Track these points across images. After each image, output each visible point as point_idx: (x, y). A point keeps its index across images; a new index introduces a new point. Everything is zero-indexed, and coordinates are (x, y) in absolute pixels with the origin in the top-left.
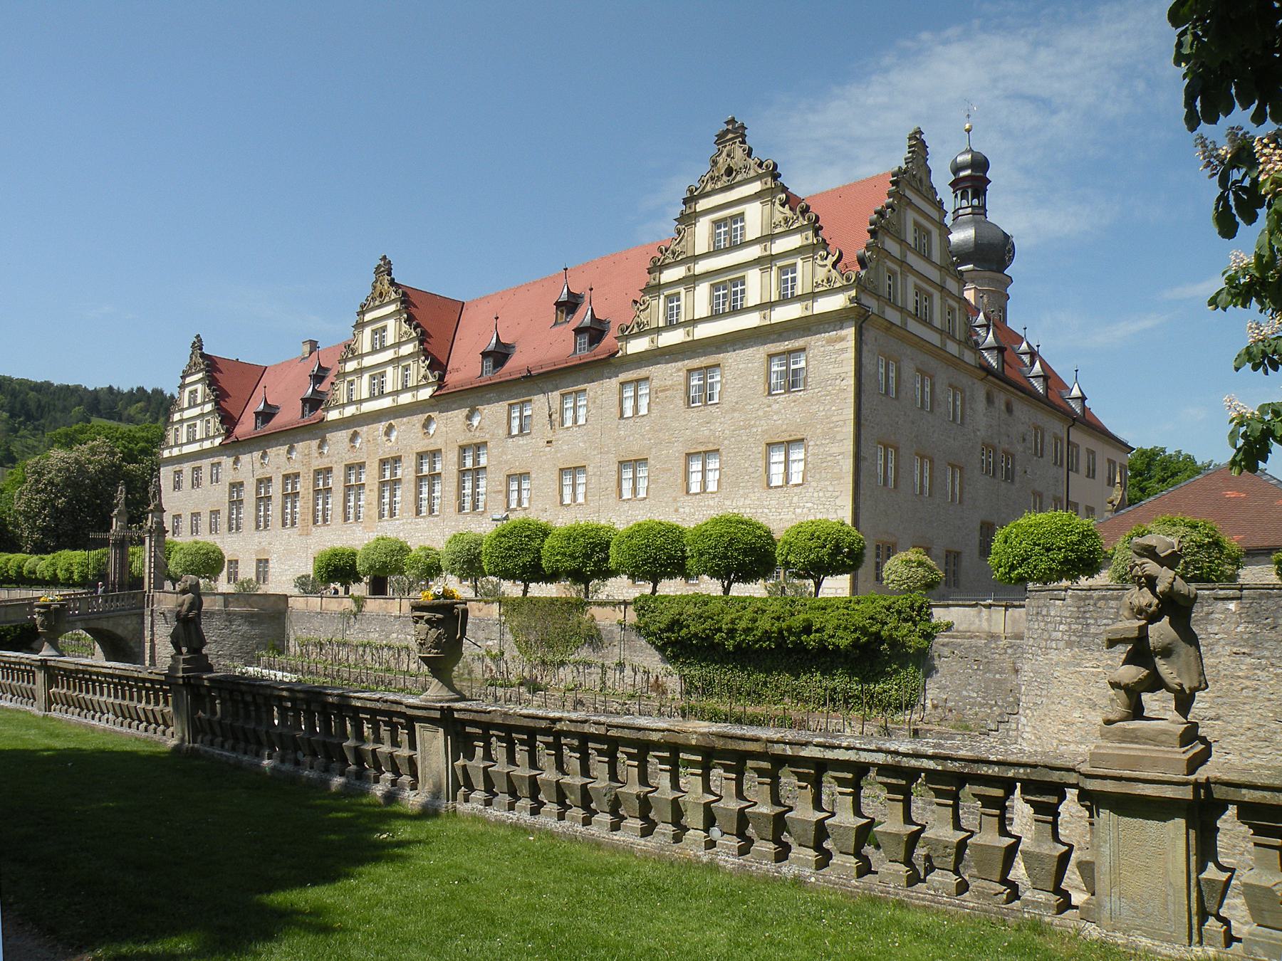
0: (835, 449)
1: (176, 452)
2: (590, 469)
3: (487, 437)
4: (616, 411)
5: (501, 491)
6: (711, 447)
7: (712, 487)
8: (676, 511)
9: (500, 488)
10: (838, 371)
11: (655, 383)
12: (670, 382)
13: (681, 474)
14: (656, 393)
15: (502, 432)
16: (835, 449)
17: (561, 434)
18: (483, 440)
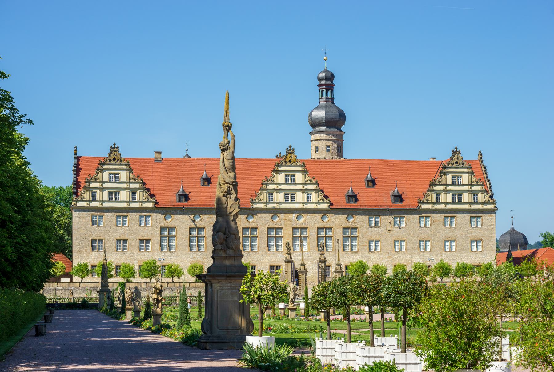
0: (491, 243)
1: (84, 204)
2: (407, 241)
3: (358, 226)
4: (418, 224)
5: (366, 245)
6: (453, 239)
7: (454, 250)
8: (442, 256)
9: (365, 244)
10: (491, 224)
11: (433, 218)
12: (438, 219)
13: (443, 245)
14: (433, 221)
15: (366, 225)
16: (491, 243)
17: (394, 229)
18: (356, 227)
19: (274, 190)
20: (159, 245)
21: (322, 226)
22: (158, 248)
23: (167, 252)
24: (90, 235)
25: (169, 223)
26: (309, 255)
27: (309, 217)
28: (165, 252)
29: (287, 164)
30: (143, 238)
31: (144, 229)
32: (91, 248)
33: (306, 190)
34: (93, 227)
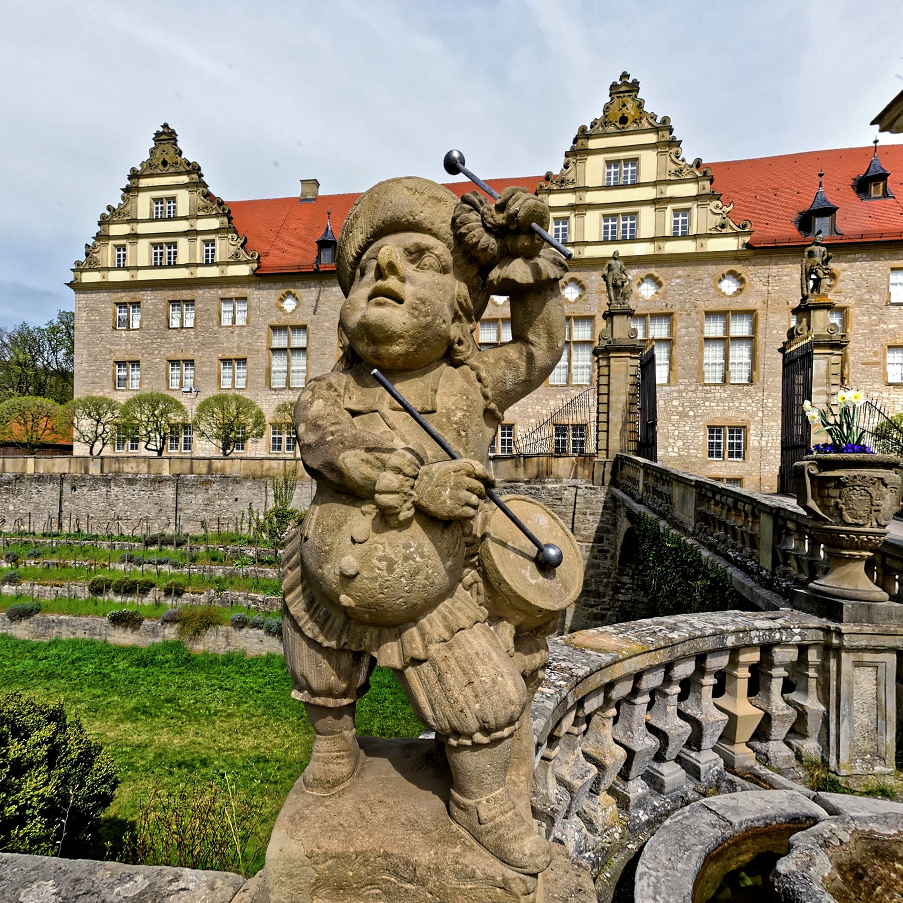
9: (874, 359)
19: (573, 207)
20: (263, 371)
21: (721, 308)
22: (262, 380)
23: (284, 389)
24: (111, 351)
25: (290, 316)
26: (675, 394)
27: (678, 281)
28: (281, 389)
29: (611, 129)
30: (228, 355)
31: (232, 332)
32: (111, 384)
33: (672, 200)
34: (116, 334)
